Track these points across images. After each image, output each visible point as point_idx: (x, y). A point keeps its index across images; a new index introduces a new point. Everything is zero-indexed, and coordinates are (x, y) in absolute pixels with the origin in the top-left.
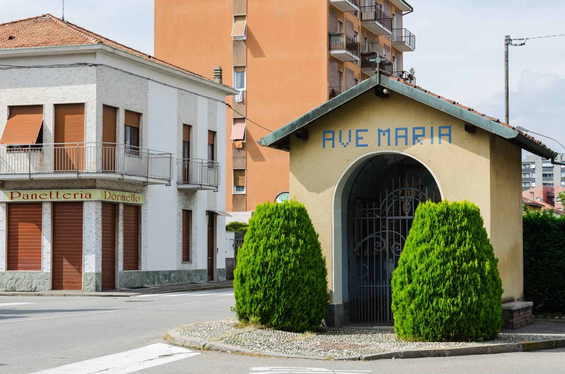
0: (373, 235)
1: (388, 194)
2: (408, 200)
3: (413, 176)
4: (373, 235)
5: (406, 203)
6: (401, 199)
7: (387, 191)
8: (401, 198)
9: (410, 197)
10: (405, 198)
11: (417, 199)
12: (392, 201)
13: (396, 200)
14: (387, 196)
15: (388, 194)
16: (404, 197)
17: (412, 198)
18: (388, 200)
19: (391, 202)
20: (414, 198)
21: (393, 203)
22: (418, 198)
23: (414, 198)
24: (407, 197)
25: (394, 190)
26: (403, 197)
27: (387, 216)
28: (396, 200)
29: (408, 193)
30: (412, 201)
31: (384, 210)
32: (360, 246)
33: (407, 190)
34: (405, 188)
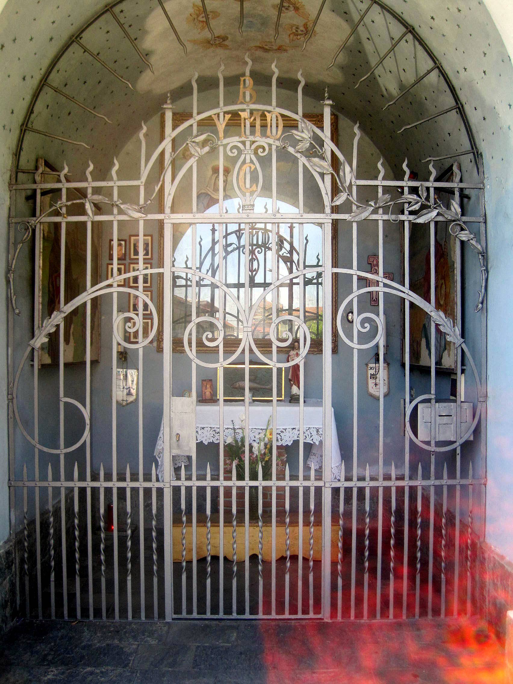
0: (110, 286)
1: (174, 128)
2: (256, 153)
3: (273, 66)
4: (110, 286)
5: (244, 162)
6: (225, 146)
7: (169, 116)
8: (225, 141)
9: (262, 141)
10: (244, 143)
11: (291, 150)
12: (191, 156)
13: (207, 149)
14: (170, 133)
15: (174, 128)
16: (237, 139)
17: (270, 145)
18: (174, 149)
19: (186, 156)
20: (278, 143)
21: (192, 162)
22: (295, 143)
23: (278, 143)
24: (252, 138)
25: (198, 113)
26: (234, 141)
27: (167, 210)
28: (207, 149)
29: (253, 126)
30: (270, 154)
31: (157, 189)
32: (58, 326)
33: (252, 112)
34: (244, 107)
